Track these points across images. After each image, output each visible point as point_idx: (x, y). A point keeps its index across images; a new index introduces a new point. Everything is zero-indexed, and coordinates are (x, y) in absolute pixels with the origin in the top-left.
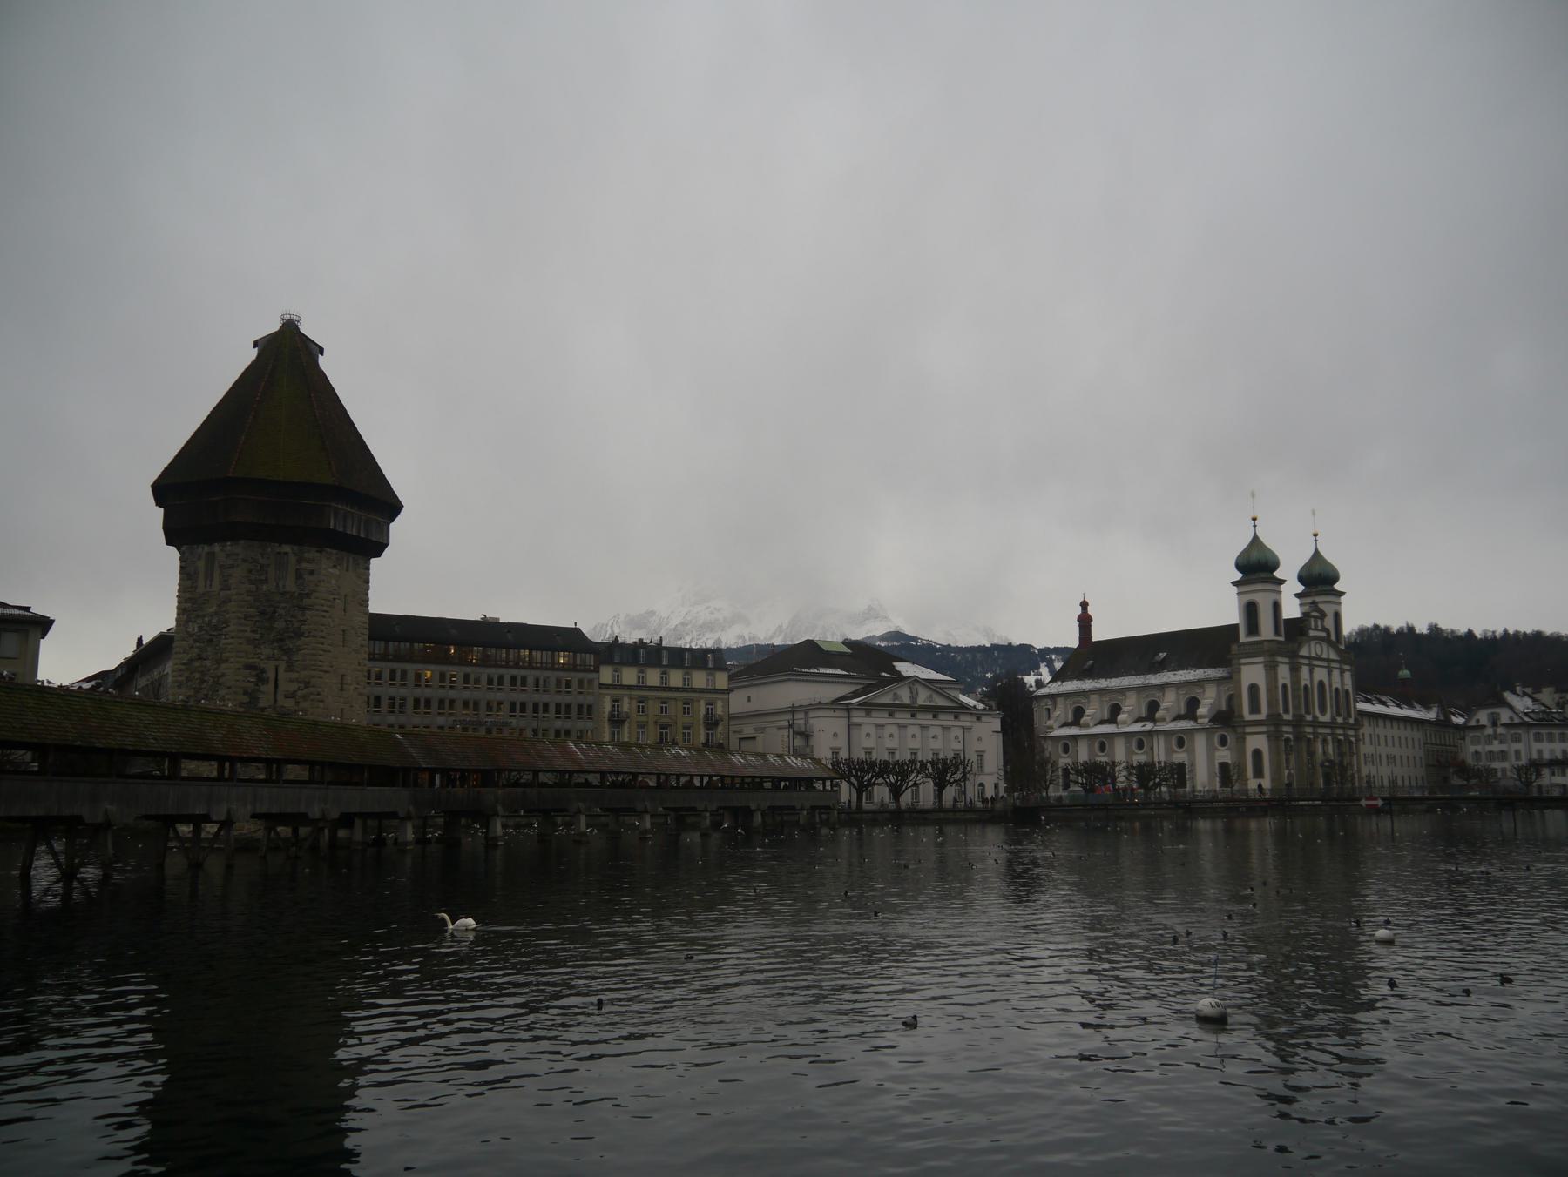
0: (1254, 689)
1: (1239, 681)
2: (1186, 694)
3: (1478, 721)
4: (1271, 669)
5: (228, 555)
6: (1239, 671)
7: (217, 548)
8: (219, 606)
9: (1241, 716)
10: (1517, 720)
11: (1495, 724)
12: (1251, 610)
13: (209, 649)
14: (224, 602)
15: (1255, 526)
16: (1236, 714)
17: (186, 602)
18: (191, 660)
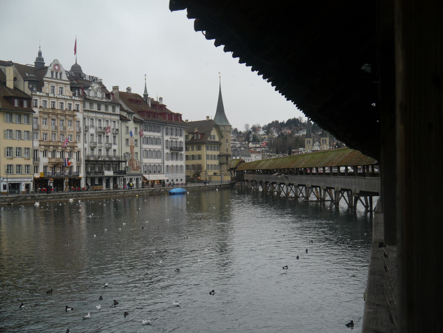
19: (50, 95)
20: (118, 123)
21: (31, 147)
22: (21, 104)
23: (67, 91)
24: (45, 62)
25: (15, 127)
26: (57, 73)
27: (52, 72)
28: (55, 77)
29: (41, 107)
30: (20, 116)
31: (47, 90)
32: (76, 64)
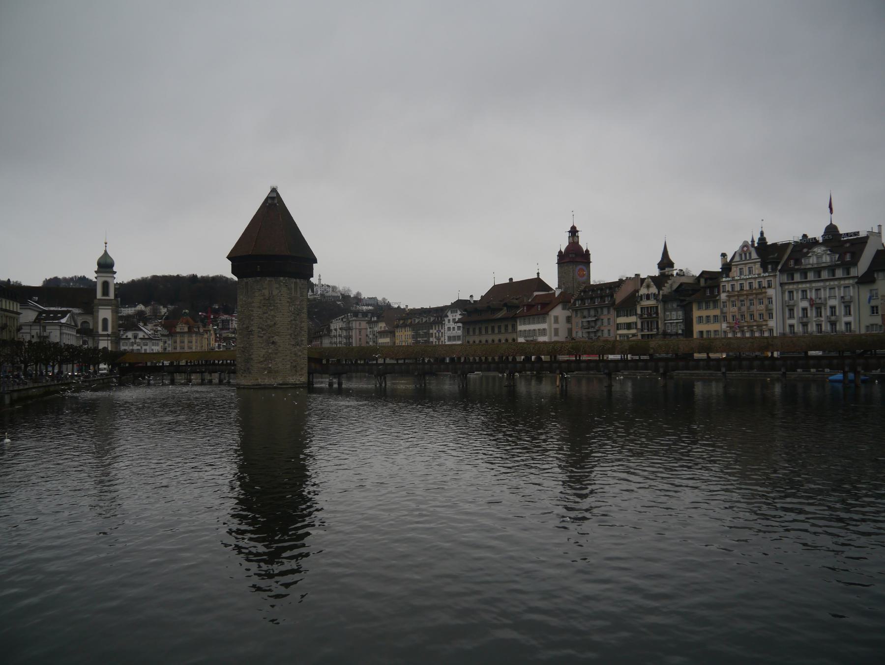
0: (105, 321)
1: (98, 317)
2: (82, 319)
3: (127, 336)
4: (115, 312)
5: (302, 284)
6: (98, 312)
7: (298, 280)
8: (300, 302)
9: (98, 332)
10: (146, 337)
11: (135, 337)
12: (106, 285)
13: (298, 317)
14: (302, 301)
15: (106, 246)
16: (95, 331)
17: (288, 298)
18: (291, 320)
19: (736, 278)
20: (854, 287)
21: (719, 329)
22: (712, 292)
23: (757, 269)
24: (767, 240)
25: (704, 313)
26: (745, 255)
27: (741, 255)
28: (743, 259)
29: (728, 291)
30: (707, 303)
31: (735, 273)
32: (831, 224)
